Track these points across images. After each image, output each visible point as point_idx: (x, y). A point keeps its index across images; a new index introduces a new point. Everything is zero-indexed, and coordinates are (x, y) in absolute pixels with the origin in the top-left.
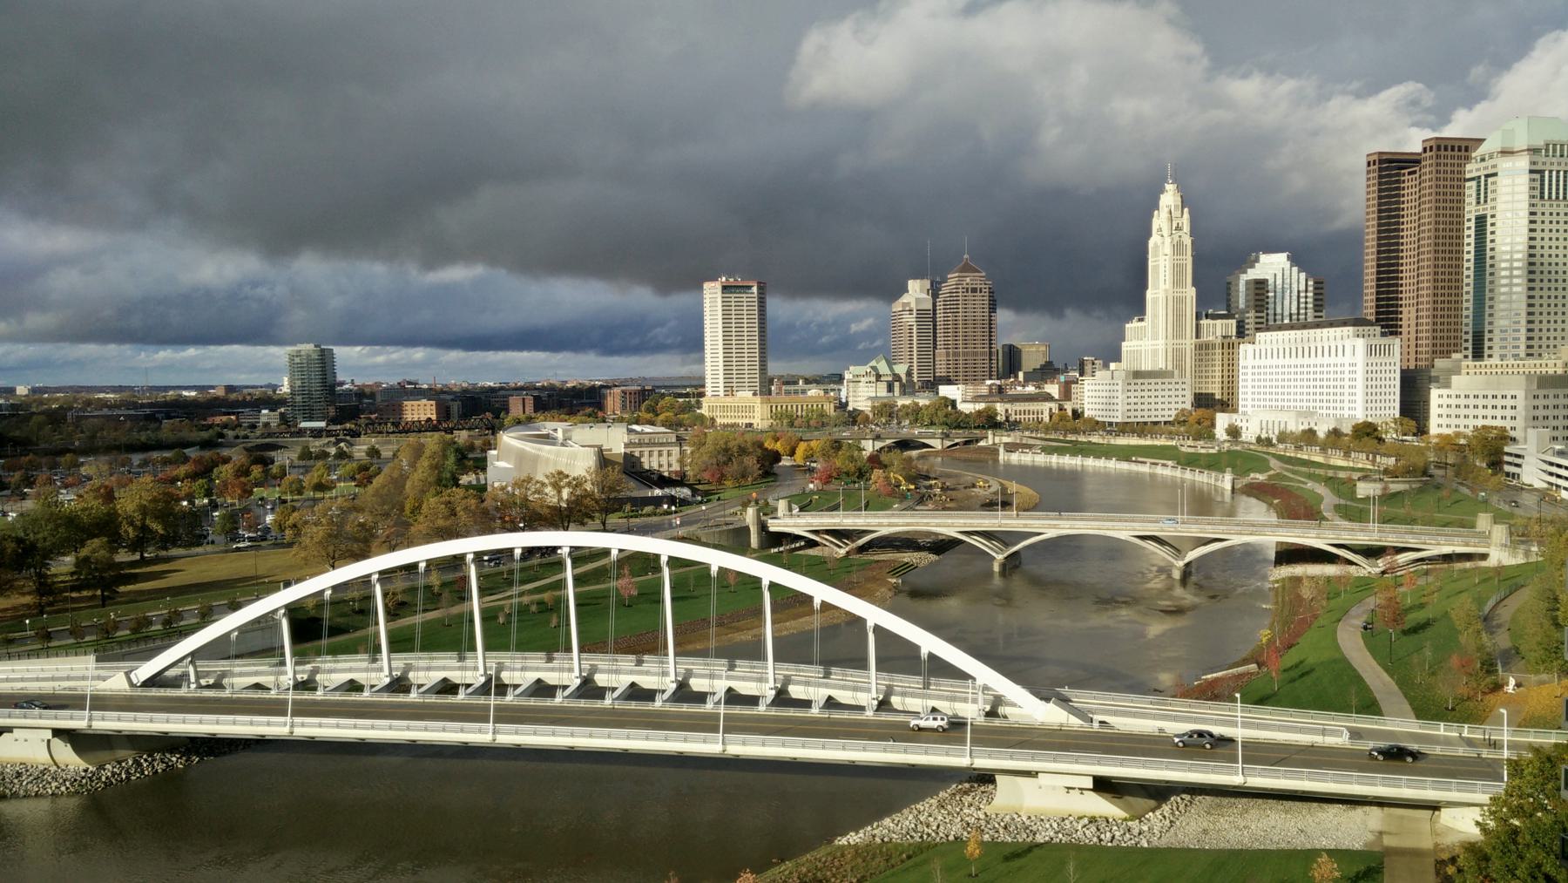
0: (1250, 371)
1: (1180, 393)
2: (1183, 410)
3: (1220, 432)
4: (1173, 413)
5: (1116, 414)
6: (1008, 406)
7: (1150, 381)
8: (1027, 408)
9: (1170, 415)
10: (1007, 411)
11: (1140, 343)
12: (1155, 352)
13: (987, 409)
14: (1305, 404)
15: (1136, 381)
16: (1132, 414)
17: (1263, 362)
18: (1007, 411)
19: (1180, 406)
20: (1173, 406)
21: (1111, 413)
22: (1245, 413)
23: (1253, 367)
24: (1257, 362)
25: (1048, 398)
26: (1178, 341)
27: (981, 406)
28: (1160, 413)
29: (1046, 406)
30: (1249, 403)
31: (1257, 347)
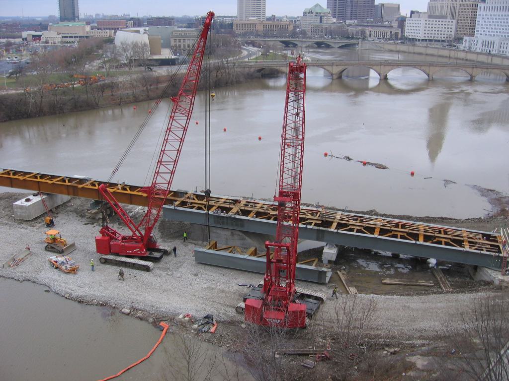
0: (481, 17)
1: (450, 27)
3: (464, 46)
4: (446, 36)
5: (420, 35)
6: (373, 30)
7: (436, 20)
9: (443, 37)
10: (370, 31)
11: (433, 3)
12: (442, 7)
14: (504, 34)
15: (430, 19)
16: (426, 35)
17: (488, 13)
18: (370, 31)
19: (449, 33)
20: (446, 33)
22: (477, 37)
23: (483, 15)
24: (485, 13)
25: (391, 27)
26: (453, 3)
28: (439, 36)
29: (388, 30)
30: (479, 33)
31: (485, 5)
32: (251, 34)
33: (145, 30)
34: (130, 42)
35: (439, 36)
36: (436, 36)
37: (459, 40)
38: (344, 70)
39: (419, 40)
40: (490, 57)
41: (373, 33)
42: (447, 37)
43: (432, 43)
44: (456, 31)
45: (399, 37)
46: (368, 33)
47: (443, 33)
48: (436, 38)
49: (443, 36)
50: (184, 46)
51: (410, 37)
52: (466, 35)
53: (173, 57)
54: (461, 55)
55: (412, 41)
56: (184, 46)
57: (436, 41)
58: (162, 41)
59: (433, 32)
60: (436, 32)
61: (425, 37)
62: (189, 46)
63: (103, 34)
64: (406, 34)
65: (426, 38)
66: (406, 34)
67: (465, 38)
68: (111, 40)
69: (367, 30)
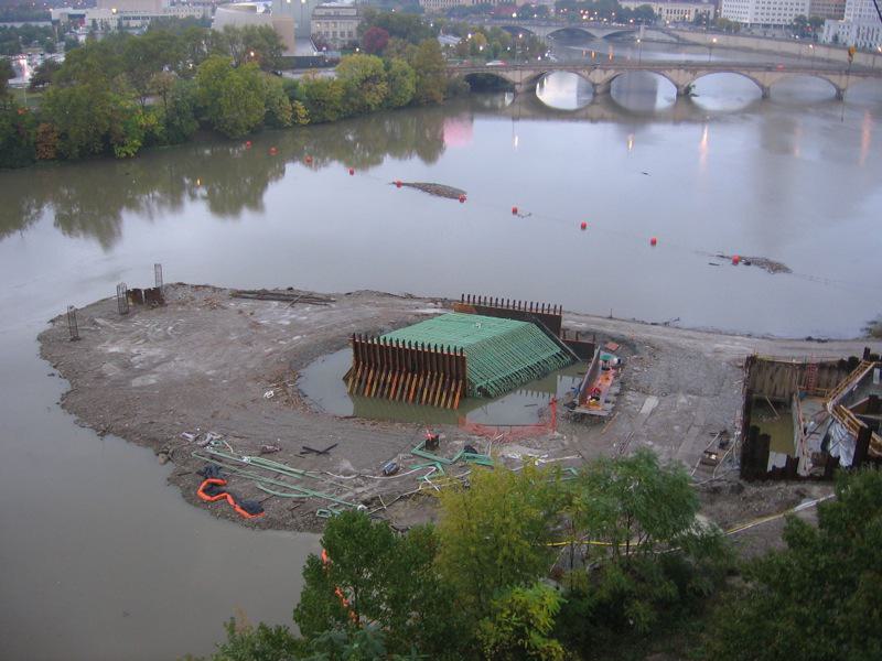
2: (801, 16)
3: (826, 35)
4: (793, 18)
6: (661, 5)
8: (677, 8)
9: (789, 19)
10: (660, 9)
13: (644, 6)
18: (660, 9)
19: (799, 13)
20: (794, 12)
21: (743, 15)
27: (642, 3)
28: (782, 18)
32: (451, 12)
33: (266, 6)
34: (239, 26)
35: (782, 18)
36: (776, 17)
37: (817, 23)
38: (613, 79)
39: (746, 24)
40: (871, 57)
41: (664, 13)
42: (796, 20)
43: (771, 30)
44: (812, 9)
45: (711, 17)
46: (656, 11)
47: (788, 12)
48: (776, 23)
49: (788, 18)
50: (335, 33)
51: (731, 20)
52: (830, 17)
53: (315, 54)
54: (821, 52)
55: (733, 28)
56: (335, 33)
57: (775, 26)
58: (296, 26)
59: (771, 11)
60: (777, 12)
61: (756, 19)
62: (342, 34)
63: (188, 13)
64: (724, 15)
65: (759, 21)
66: (724, 15)
67: (827, 22)
68: (206, 22)
69: (656, 8)
